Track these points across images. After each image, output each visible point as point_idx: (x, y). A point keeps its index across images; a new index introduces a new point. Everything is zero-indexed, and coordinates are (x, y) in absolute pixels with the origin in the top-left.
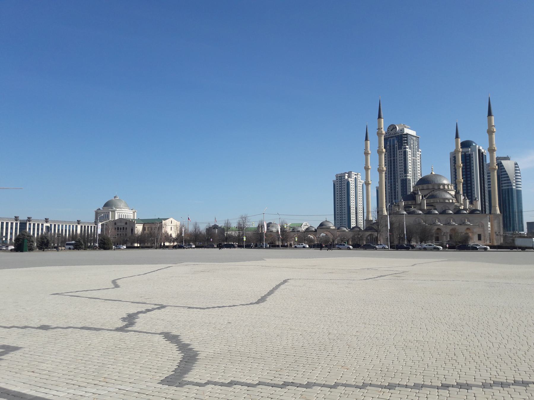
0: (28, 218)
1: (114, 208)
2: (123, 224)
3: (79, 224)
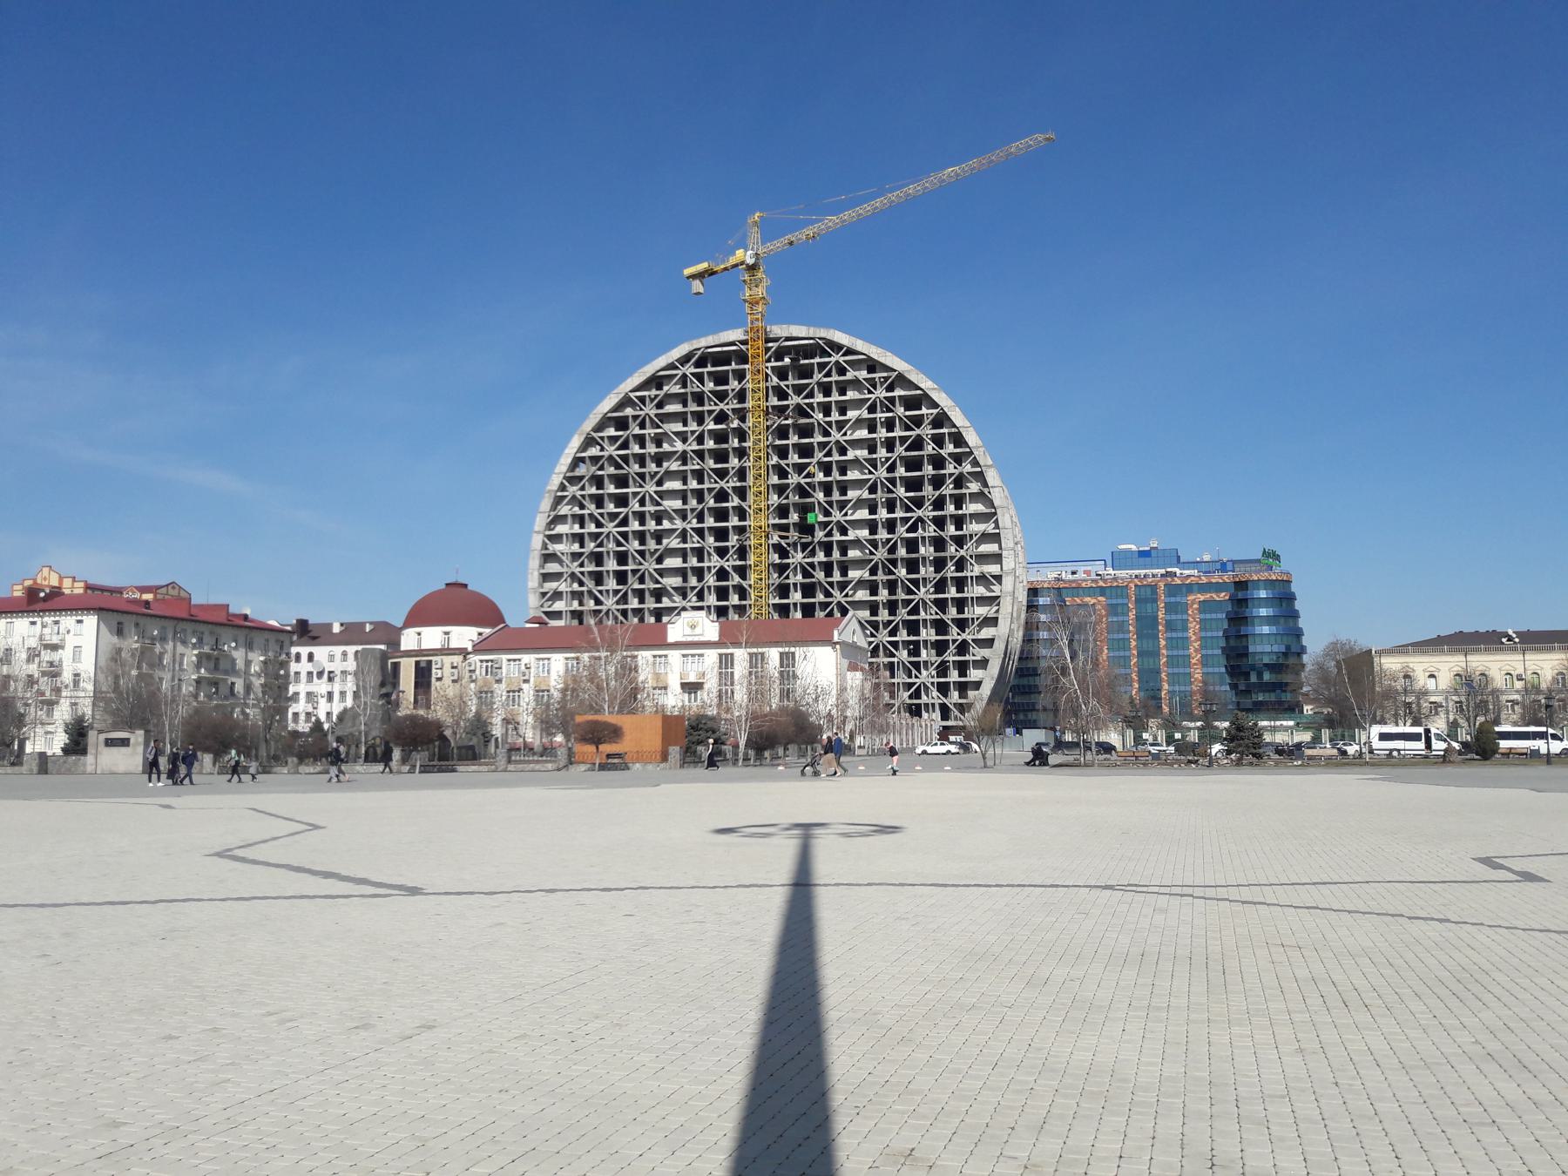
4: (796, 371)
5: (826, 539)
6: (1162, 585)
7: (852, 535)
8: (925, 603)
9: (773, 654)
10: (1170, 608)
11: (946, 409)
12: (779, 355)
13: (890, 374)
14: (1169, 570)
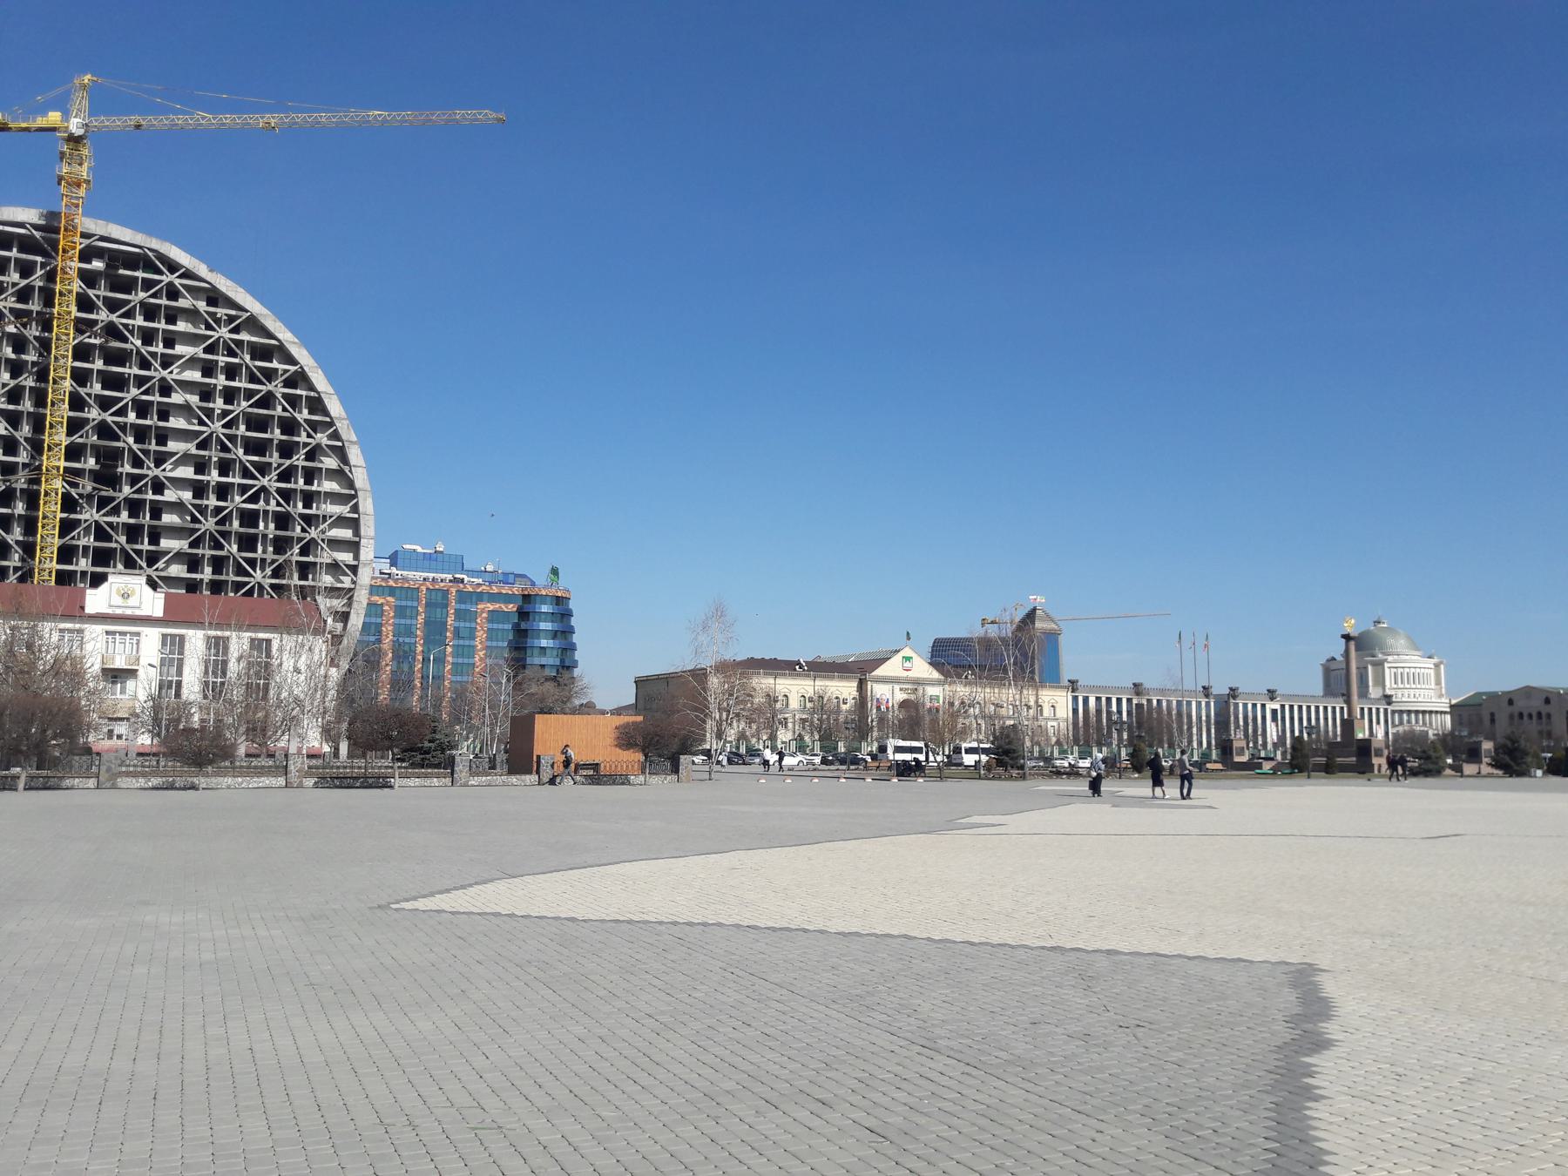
0: (1231, 689)
1: (1380, 656)
2: (1536, 704)
3: (1272, 699)
4: (108, 281)
5: (136, 496)
6: (453, 590)
7: (170, 495)
8: (261, 587)
9: (239, 642)
10: (459, 615)
11: (305, 368)
12: (86, 256)
13: (240, 313)
14: (457, 576)
